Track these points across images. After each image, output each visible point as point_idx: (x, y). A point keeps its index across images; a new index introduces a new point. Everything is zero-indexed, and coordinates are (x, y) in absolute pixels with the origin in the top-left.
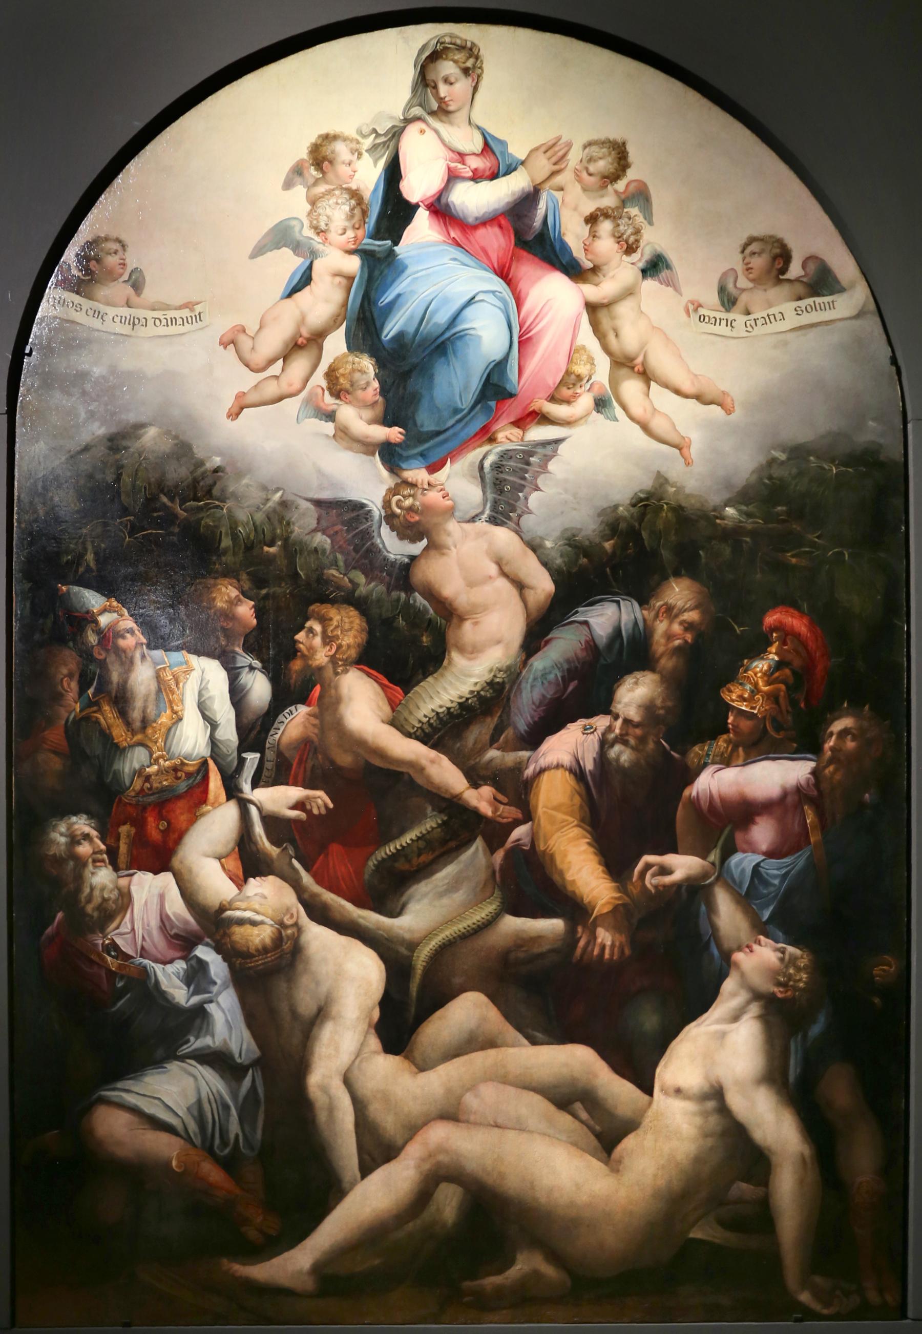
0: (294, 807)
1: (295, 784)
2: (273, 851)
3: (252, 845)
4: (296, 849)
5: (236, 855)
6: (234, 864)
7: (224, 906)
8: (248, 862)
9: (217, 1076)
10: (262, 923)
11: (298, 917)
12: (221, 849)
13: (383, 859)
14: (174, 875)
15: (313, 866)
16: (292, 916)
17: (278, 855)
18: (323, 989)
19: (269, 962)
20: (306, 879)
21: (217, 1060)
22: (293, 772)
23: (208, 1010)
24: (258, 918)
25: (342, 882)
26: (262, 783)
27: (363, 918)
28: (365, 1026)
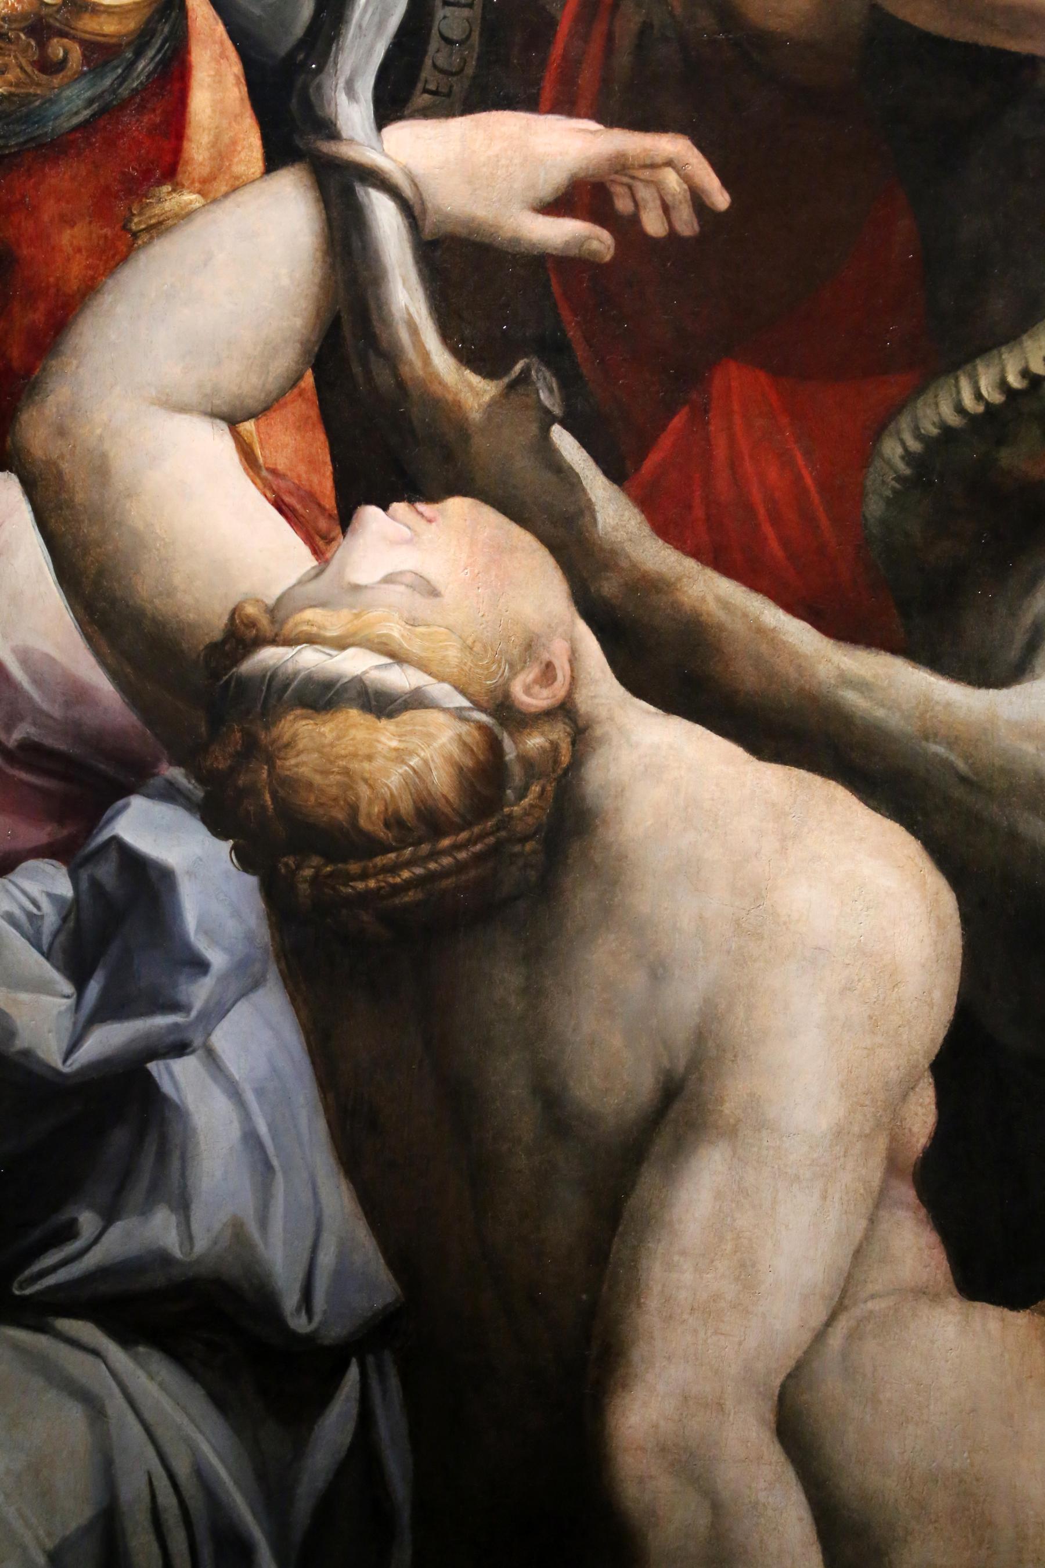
0: (558, 205)
1: (566, 106)
2: (471, 391)
3: (377, 367)
4: (570, 384)
5: (304, 407)
6: (298, 445)
7: (252, 624)
8: (358, 436)
9: (196, 1398)
10: (416, 701)
11: (573, 680)
12: (240, 378)
13: (948, 432)
14: (30, 487)
15: (642, 454)
16: (548, 672)
17: (493, 403)
18: (686, 996)
19: (444, 873)
20: (613, 513)
21: (206, 1321)
22: (557, 50)
23: (167, 1087)
24: (400, 679)
25: (768, 530)
26: (422, 99)
27: (862, 686)
28: (874, 1171)
